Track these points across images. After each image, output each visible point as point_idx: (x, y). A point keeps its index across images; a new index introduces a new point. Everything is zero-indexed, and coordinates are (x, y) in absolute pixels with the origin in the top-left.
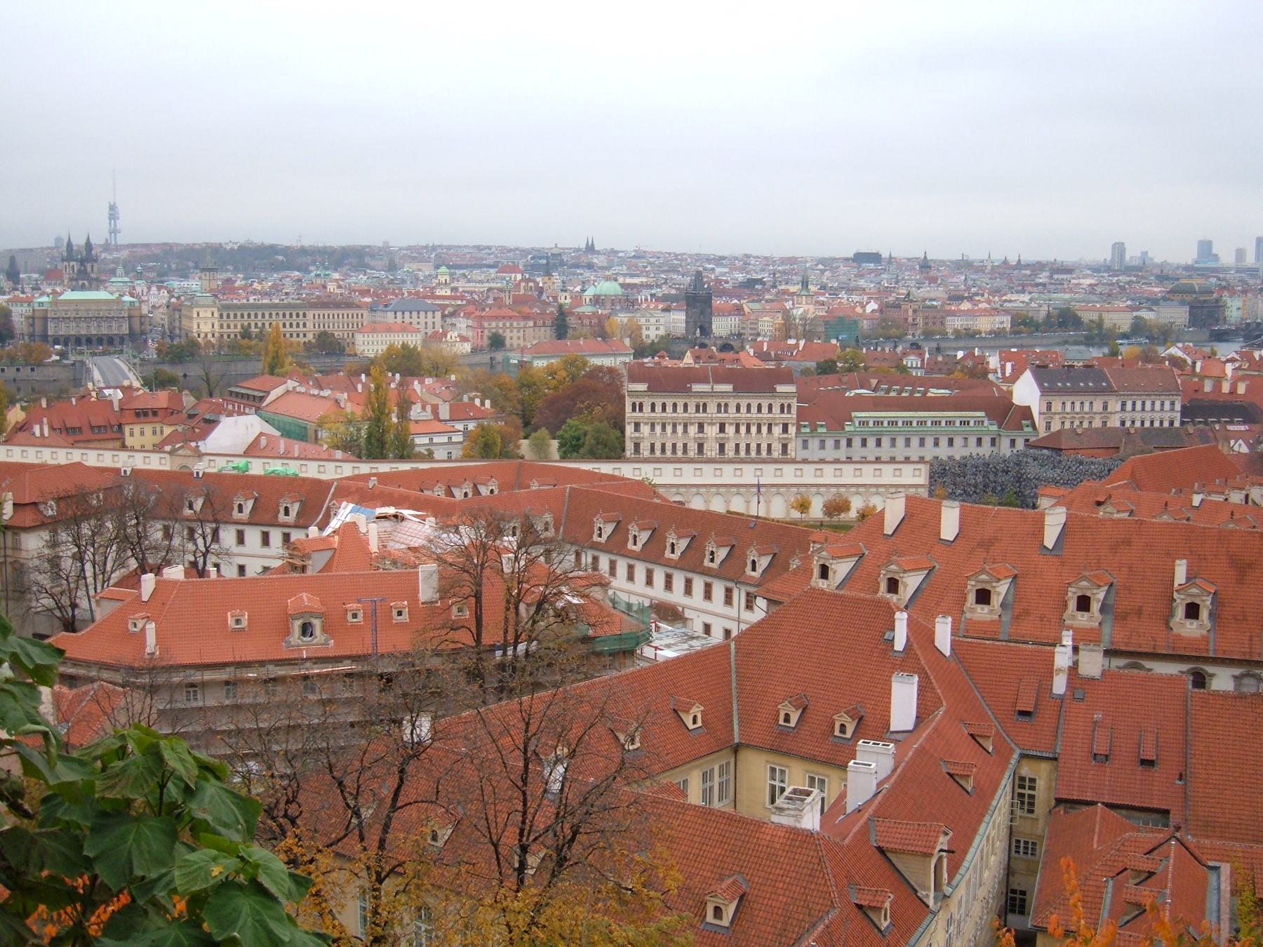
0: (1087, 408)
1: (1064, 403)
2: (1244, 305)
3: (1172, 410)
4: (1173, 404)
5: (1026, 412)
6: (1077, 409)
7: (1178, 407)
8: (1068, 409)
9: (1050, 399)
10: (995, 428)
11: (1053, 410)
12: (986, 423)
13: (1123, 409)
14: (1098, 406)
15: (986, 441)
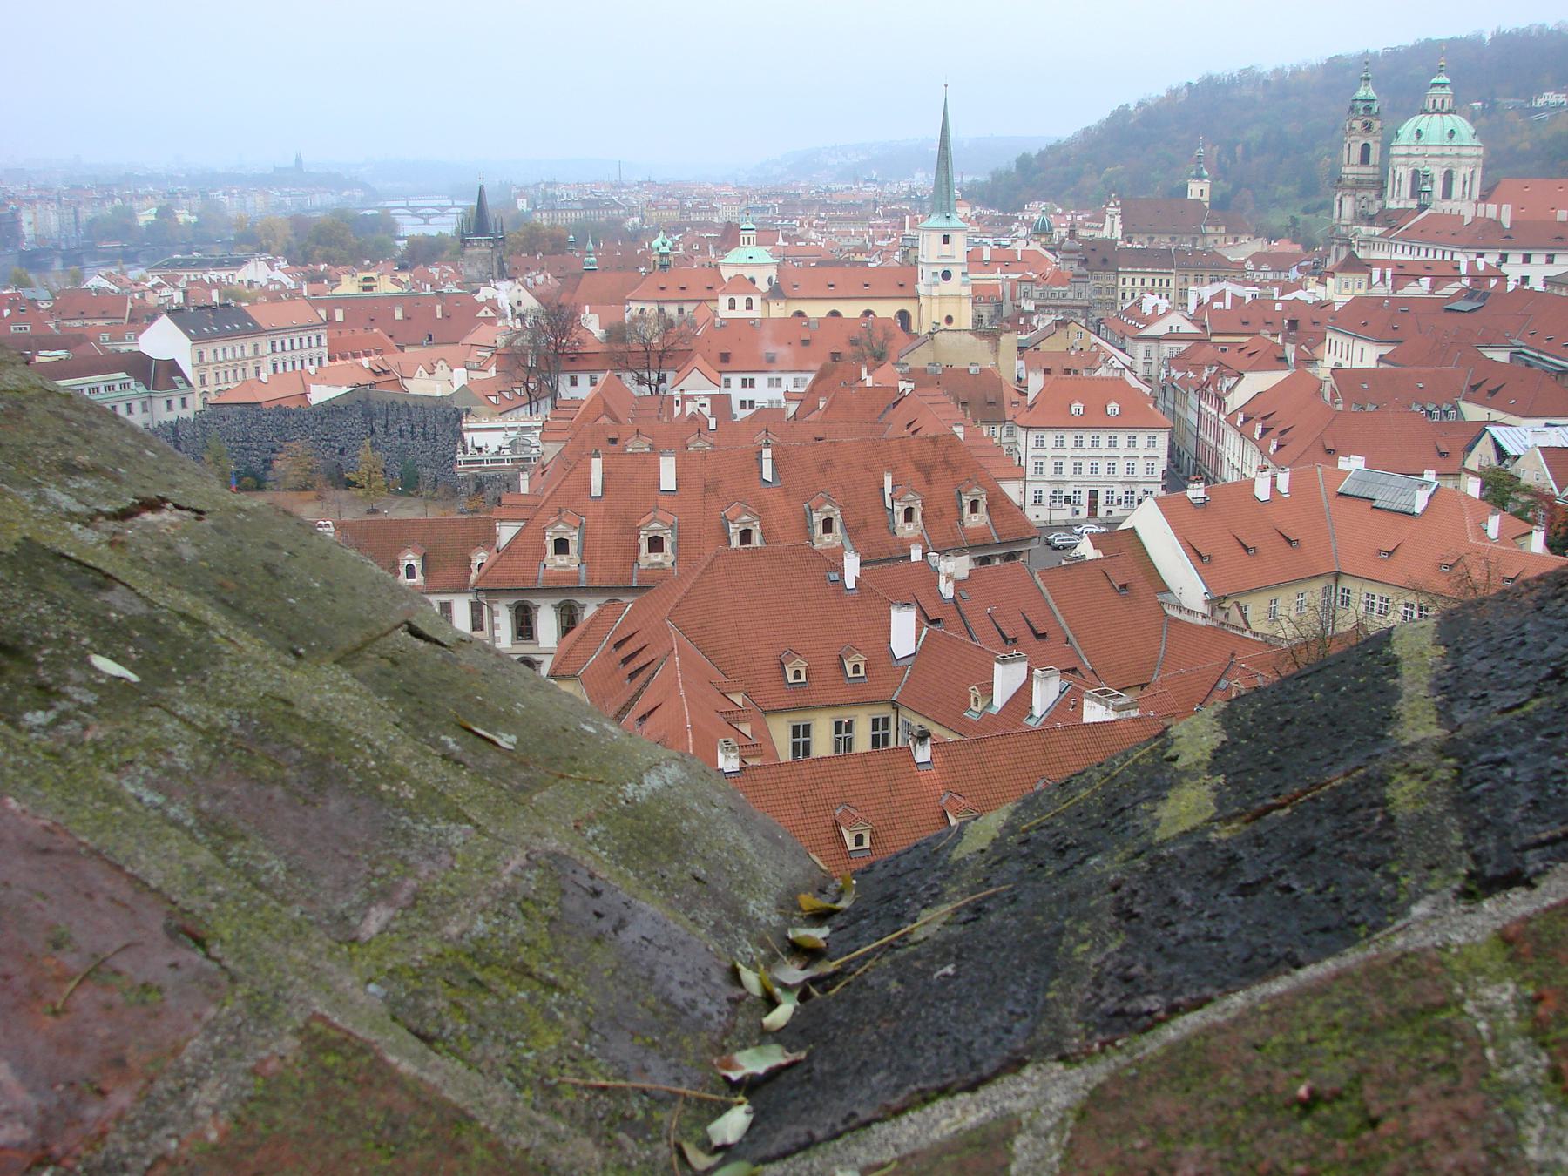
0: (238, 354)
1: (215, 351)
2: (35, 219)
3: (319, 345)
4: (319, 338)
5: (172, 367)
6: (230, 356)
7: (324, 341)
8: (220, 357)
9: (201, 347)
10: (142, 389)
11: (206, 361)
12: (133, 385)
13: (274, 351)
14: (249, 351)
15: (137, 405)
